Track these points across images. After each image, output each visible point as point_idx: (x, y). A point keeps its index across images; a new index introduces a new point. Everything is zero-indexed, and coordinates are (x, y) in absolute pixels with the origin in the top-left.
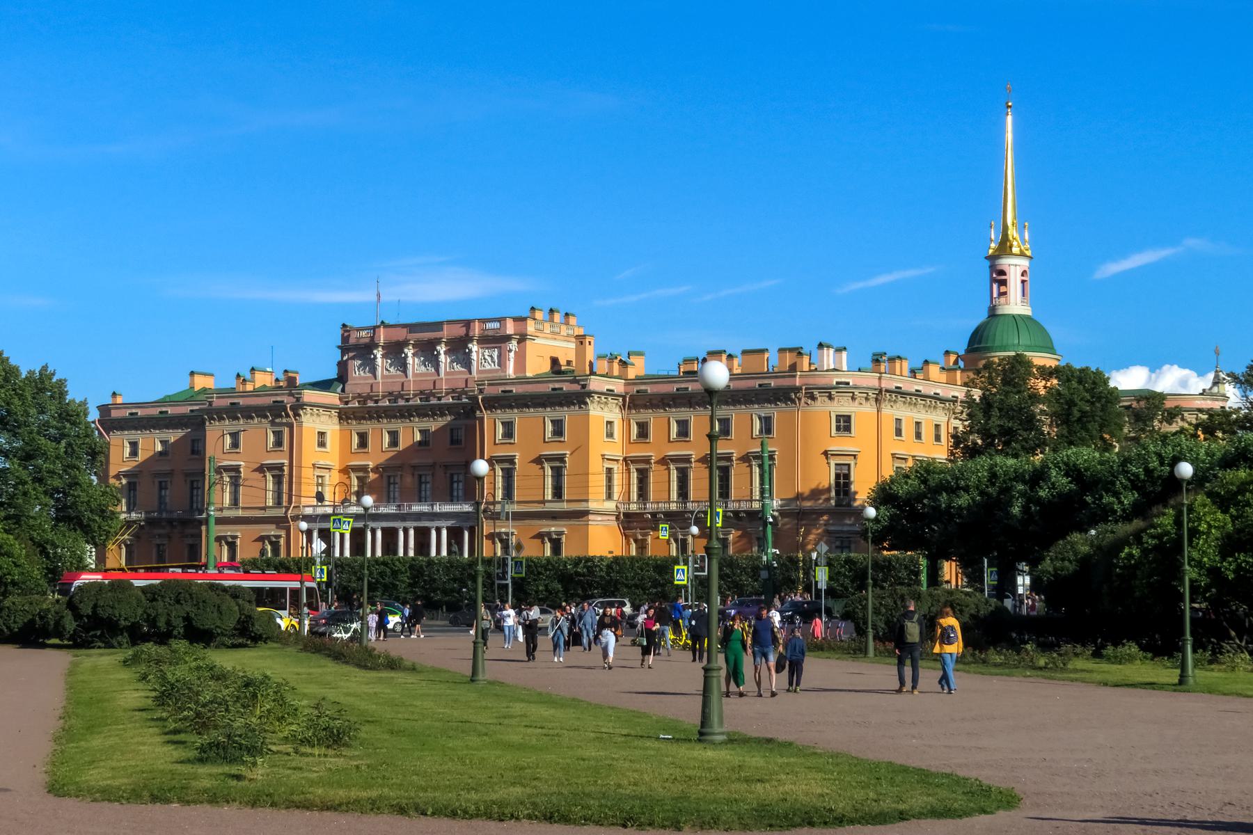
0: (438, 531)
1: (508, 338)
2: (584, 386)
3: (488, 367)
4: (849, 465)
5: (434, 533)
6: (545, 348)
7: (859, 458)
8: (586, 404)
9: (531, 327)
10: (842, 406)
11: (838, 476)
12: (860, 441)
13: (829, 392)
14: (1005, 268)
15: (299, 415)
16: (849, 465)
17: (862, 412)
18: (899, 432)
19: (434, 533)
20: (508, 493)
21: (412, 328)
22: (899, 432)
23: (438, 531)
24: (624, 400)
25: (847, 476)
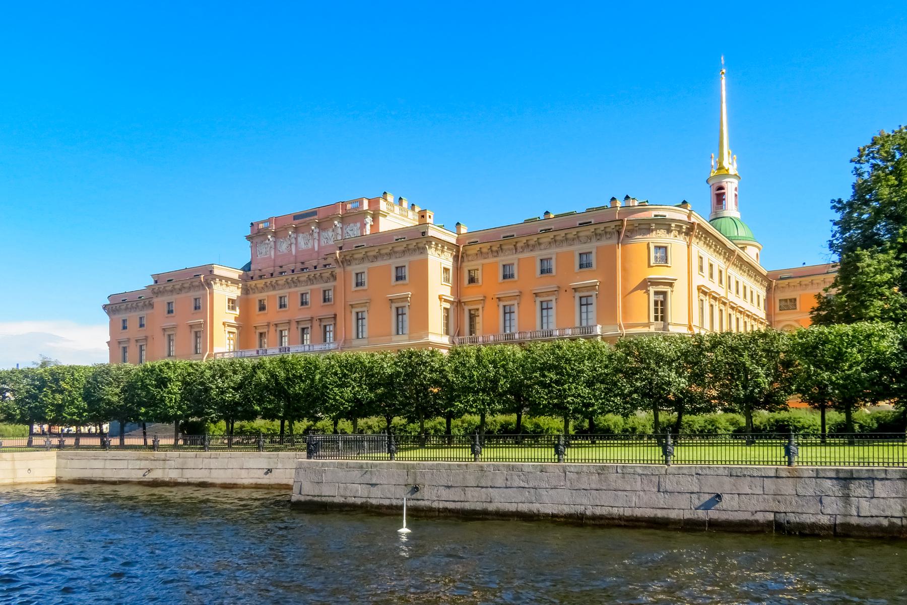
1: (365, 213)
2: (424, 233)
4: (664, 294)
6: (395, 219)
7: (676, 284)
8: (424, 248)
9: (383, 205)
10: (660, 237)
11: (656, 303)
12: (676, 269)
13: (646, 227)
14: (724, 184)
15: (211, 284)
16: (664, 294)
17: (676, 243)
18: (701, 268)
21: (296, 217)
22: (701, 268)
24: (458, 251)
25: (663, 303)
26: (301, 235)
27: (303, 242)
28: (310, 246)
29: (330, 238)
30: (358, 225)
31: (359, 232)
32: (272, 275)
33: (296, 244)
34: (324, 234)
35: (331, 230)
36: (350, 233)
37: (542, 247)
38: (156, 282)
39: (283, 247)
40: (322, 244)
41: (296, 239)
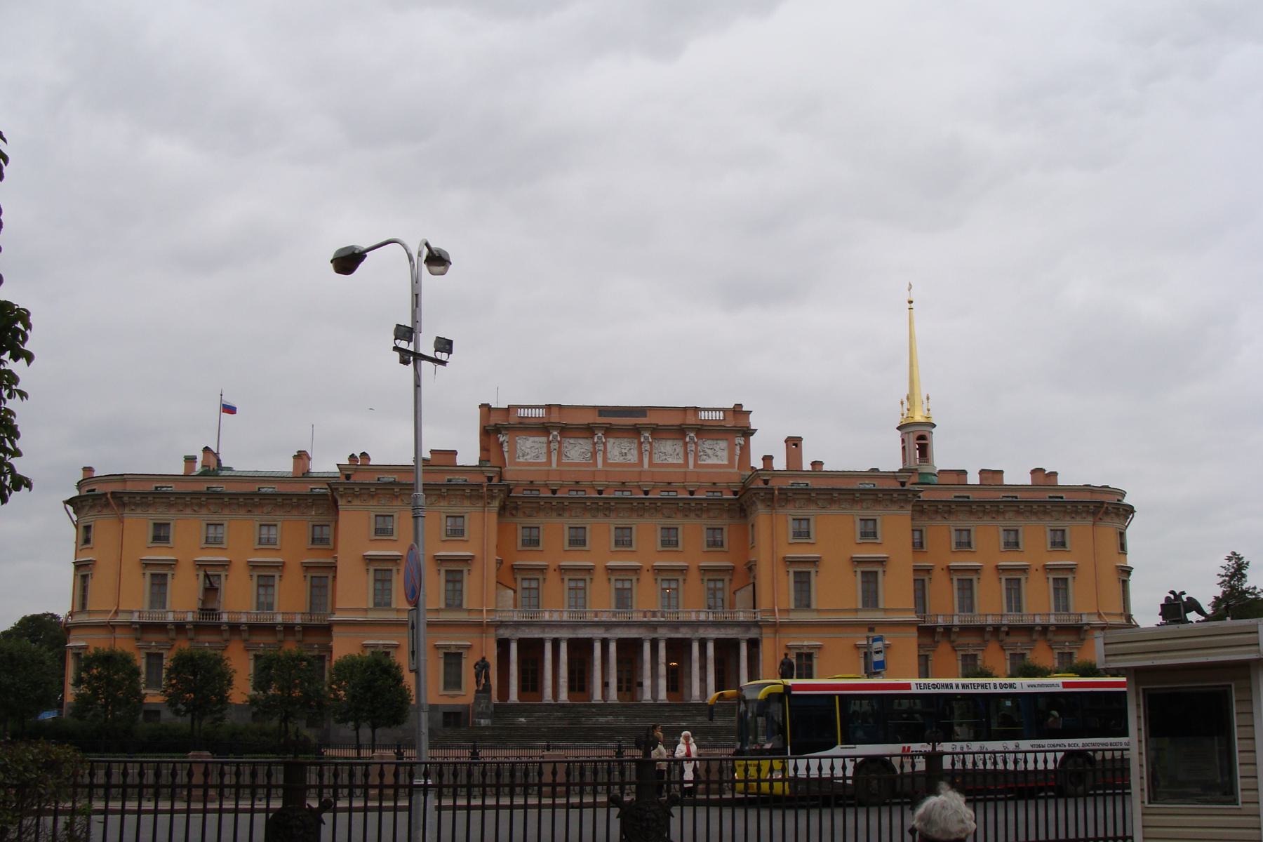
0: (703, 644)
3: (709, 462)
5: (695, 647)
19: (695, 647)
20: (804, 601)
21: (603, 411)
23: (703, 644)
26: (611, 441)
27: (619, 452)
28: (633, 457)
29: (669, 453)
30: (723, 444)
31: (725, 454)
32: (554, 492)
33: (605, 452)
34: (656, 445)
35: (669, 443)
36: (709, 452)
37: (1007, 516)
38: (348, 477)
39: (577, 451)
40: (656, 461)
41: (605, 444)
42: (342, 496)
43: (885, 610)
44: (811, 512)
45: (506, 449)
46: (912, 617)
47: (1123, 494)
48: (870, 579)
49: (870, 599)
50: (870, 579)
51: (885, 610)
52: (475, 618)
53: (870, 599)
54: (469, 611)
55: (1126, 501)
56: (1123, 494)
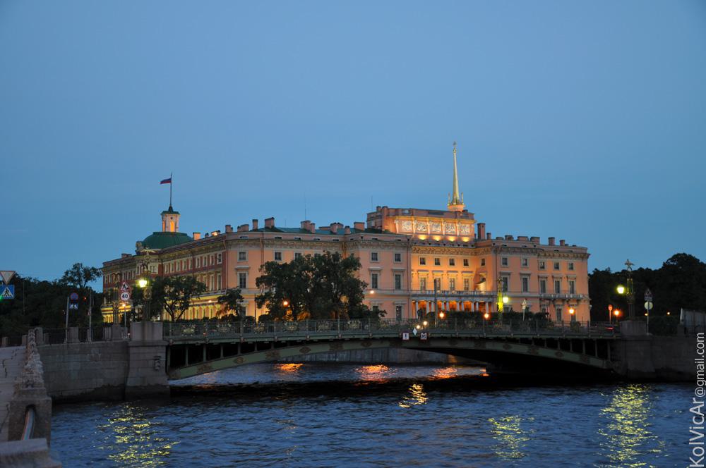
30: (468, 226)
42: (361, 245)
43: (530, 292)
44: (508, 256)
45: (397, 225)
46: (537, 295)
47: (586, 249)
48: (525, 281)
49: (526, 289)
50: (525, 281)
51: (530, 292)
52: (406, 293)
53: (526, 289)
54: (404, 290)
55: (588, 252)
56: (586, 249)
